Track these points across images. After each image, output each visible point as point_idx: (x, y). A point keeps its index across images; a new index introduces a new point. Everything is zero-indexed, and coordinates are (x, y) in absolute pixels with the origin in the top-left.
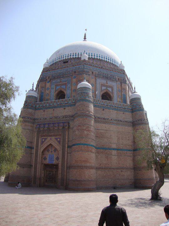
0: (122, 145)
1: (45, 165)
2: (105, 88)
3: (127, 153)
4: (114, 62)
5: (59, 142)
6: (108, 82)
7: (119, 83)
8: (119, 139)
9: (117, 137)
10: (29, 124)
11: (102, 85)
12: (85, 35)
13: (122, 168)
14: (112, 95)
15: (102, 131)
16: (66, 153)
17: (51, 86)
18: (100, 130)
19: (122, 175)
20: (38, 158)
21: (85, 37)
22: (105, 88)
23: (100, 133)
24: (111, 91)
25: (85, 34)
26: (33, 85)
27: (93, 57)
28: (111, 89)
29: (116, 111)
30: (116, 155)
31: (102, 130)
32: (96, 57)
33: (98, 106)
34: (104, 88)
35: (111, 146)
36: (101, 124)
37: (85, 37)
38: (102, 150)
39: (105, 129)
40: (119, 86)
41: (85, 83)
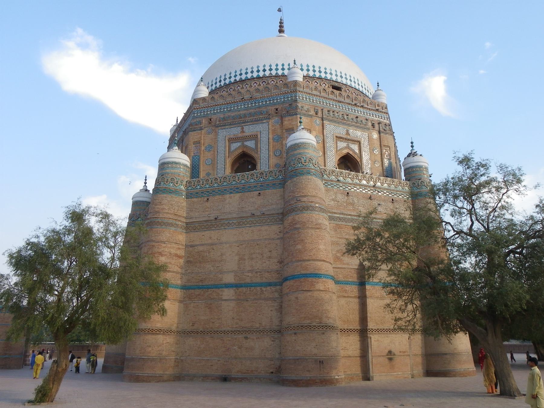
0: (250, 274)
3: (262, 291)
6: (246, 128)
7: (275, 120)
8: (242, 259)
11: (232, 140)
12: (281, 23)
13: (246, 332)
15: (201, 248)
18: (197, 245)
19: (247, 348)
21: (281, 26)
22: (239, 144)
28: (253, 142)
29: (238, 195)
30: (233, 298)
31: (202, 245)
33: (197, 195)
35: (221, 280)
36: (199, 233)
38: (197, 292)
39: (210, 241)
40: (278, 126)
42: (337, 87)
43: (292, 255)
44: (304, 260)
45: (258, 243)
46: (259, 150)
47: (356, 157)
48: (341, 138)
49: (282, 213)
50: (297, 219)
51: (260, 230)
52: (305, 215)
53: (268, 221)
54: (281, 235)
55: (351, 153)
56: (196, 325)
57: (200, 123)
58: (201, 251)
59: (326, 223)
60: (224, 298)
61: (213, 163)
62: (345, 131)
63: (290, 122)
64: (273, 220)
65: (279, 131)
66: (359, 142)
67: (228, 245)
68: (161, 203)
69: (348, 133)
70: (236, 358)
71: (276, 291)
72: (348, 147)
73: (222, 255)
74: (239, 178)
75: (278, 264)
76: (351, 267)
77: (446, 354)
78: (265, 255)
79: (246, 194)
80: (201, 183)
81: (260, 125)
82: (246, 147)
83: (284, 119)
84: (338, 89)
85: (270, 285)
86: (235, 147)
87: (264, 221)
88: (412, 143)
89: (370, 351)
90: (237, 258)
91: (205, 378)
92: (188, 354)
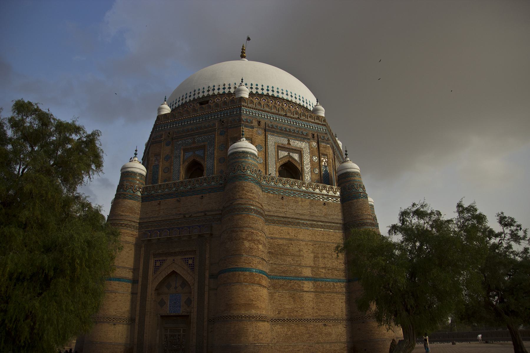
0: (323, 271)
1: (161, 316)
3: (334, 286)
4: (303, 101)
5: (192, 267)
6: (292, 142)
9: (313, 252)
10: (128, 231)
11: (280, 147)
12: (243, 49)
13: (325, 320)
15: (281, 242)
16: (207, 288)
18: (277, 238)
19: (326, 334)
22: (286, 154)
23: (278, 245)
26: (136, 151)
27: (260, 92)
30: (312, 290)
32: (265, 92)
35: (301, 273)
38: (281, 282)
39: (288, 237)
41: (245, 145)
56: (282, 313)
57: (252, 122)
58: (281, 245)
60: (305, 289)
67: (304, 243)
70: (318, 343)
73: (300, 251)
85: (340, 282)
90: (312, 255)
92: (276, 341)
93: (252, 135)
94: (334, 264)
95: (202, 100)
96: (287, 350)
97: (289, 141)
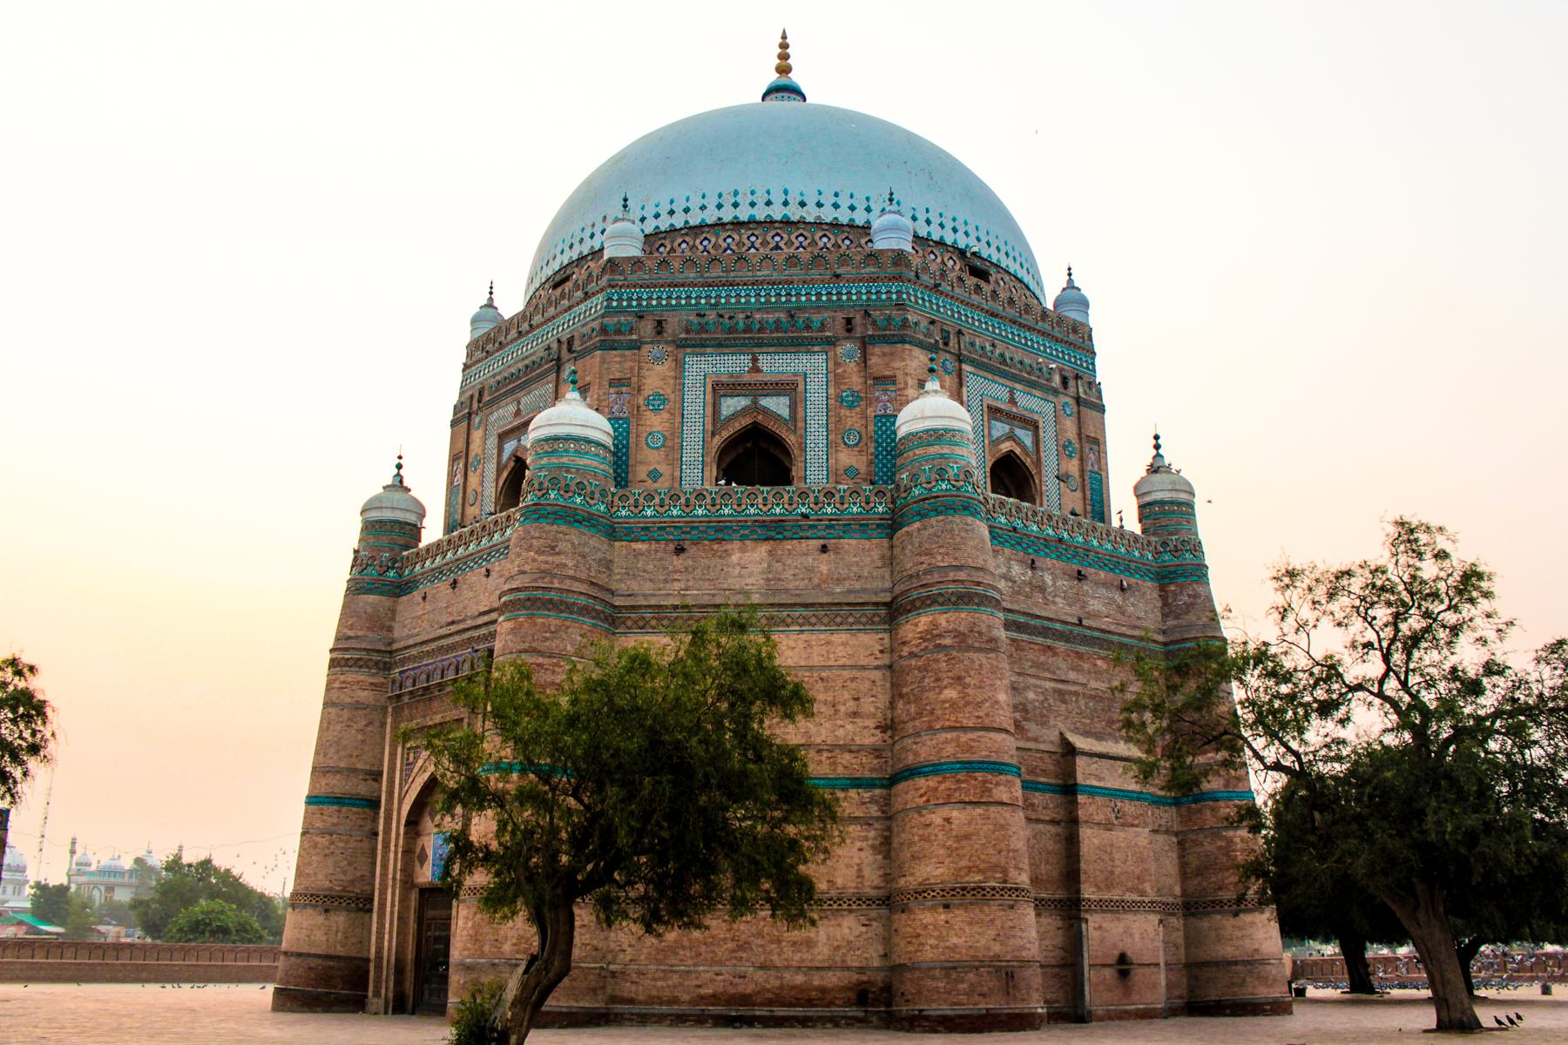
2: (740, 403)
6: (765, 362)
7: (847, 348)
11: (722, 388)
12: (784, 46)
14: (791, 439)
17: (485, 439)
20: (392, 855)
21: (784, 57)
22: (740, 403)
24: (785, 413)
25: (784, 37)
28: (785, 400)
34: (731, 405)
37: (784, 57)
40: (852, 367)
42: (979, 269)
43: (932, 712)
44: (964, 729)
45: (824, 674)
46: (800, 424)
47: (1028, 462)
48: (998, 410)
49: (887, 605)
50: (944, 624)
51: (828, 643)
52: (963, 615)
53: (851, 620)
54: (886, 659)
55: (1018, 451)
59: (1002, 634)
61: (673, 447)
62: (1006, 396)
63: (886, 359)
64: (864, 620)
65: (856, 381)
66: (1034, 426)
68: (553, 548)
69: (1012, 401)
71: (872, 801)
72: (1011, 437)
74: (765, 499)
75: (878, 732)
76: (1042, 747)
77: (1236, 963)
78: (842, 709)
79: (788, 545)
80: (657, 500)
81: (804, 358)
82: (766, 411)
83: (870, 349)
84: (981, 274)
86: (731, 410)
87: (839, 620)
88: (1156, 437)
89: (1086, 955)
91: (680, 1020)
93: (632, 369)
94: (840, 733)
95: (558, 278)
96: (660, 984)
97: (755, 360)
